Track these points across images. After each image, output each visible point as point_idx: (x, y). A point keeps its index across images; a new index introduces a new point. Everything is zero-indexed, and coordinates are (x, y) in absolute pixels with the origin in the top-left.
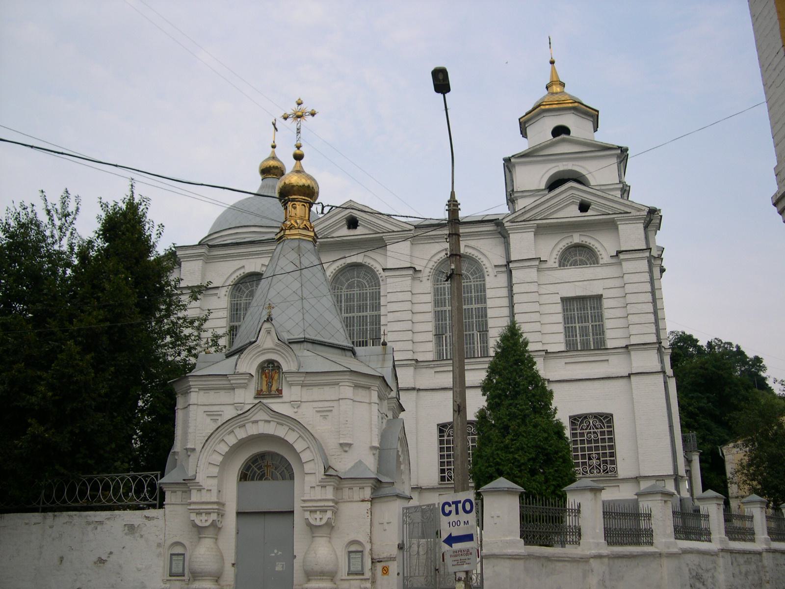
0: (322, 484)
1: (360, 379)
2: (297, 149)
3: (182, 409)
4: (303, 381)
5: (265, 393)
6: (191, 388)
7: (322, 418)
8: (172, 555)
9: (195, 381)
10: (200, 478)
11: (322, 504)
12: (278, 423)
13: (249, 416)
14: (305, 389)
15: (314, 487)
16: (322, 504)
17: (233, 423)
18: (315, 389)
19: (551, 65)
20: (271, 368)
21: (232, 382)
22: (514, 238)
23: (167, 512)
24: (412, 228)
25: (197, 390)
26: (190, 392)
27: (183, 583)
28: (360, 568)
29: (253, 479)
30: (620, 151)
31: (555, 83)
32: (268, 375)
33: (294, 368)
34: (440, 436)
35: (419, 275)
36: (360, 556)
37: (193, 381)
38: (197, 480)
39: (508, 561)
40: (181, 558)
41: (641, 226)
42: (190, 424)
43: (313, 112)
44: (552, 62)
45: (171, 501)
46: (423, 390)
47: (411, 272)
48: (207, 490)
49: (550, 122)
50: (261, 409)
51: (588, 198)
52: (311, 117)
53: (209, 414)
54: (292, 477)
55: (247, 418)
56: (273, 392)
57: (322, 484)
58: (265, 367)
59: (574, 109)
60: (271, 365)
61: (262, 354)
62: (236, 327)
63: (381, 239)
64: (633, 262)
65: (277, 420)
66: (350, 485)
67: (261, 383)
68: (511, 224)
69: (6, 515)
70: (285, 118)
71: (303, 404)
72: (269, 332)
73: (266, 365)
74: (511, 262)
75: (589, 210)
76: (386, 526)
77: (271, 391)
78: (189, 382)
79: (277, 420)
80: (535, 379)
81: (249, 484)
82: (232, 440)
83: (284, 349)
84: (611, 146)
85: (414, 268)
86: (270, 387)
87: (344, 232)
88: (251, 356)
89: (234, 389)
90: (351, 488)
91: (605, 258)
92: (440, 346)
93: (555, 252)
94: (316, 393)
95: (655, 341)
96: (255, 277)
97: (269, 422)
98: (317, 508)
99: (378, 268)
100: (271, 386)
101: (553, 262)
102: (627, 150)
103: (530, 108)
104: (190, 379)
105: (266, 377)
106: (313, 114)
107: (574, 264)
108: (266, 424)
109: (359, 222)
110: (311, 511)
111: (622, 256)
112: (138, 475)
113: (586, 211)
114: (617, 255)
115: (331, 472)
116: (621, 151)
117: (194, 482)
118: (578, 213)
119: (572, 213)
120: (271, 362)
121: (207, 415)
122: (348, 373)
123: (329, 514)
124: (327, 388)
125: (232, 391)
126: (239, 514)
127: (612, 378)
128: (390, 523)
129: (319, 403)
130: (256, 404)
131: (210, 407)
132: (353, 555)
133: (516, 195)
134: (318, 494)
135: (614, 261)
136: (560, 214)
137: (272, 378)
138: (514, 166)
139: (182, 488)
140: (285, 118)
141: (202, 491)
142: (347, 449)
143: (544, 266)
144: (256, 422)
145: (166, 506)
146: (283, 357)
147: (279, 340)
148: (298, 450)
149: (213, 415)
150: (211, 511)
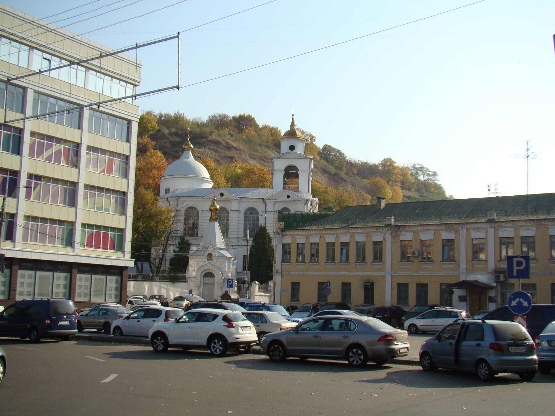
22: (268, 204)
31: (293, 125)
44: (293, 115)
63: (230, 201)
87: (220, 197)
99: (229, 209)
113: (289, 198)
115: (223, 277)
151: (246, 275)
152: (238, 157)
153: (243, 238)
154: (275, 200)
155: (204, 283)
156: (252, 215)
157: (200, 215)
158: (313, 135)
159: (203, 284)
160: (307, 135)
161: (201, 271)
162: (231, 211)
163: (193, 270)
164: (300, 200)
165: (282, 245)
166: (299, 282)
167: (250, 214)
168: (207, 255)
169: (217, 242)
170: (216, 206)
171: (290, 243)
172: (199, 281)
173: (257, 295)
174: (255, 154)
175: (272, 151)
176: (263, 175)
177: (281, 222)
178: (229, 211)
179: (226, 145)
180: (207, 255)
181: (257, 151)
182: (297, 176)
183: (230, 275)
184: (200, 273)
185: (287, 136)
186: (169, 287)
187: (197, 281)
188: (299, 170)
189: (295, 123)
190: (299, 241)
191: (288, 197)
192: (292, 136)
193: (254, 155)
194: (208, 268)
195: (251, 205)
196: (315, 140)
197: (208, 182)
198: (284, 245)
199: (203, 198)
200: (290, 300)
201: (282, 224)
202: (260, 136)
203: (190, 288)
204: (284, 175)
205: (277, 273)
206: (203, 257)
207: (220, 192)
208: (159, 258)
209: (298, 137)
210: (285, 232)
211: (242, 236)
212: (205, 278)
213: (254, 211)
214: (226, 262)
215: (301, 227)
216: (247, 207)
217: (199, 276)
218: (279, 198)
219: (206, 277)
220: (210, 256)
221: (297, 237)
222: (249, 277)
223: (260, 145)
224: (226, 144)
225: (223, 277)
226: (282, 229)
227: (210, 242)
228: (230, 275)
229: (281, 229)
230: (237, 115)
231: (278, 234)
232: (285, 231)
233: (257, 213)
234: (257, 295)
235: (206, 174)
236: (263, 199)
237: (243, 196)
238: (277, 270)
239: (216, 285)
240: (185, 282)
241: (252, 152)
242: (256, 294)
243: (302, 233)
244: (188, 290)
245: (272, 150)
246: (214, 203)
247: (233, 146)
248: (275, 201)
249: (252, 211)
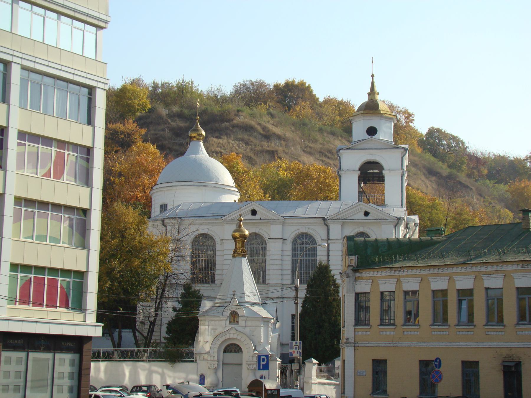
11: (253, 362)
16: (253, 362)
22: (331, 227)
31: (372, 92)
34: (292, 320)
35: (285, 241)
46: (285, 298)
47: (282, 240)
51: (368, 210)
54: (242, 351)
68: (331, 221)
85: (284, 239)
86: (234, 320)
87: (250, 217)
92: (294, 277)
99: (266, 237)
115: (256, 352)
136: (355, 217)
137: (235, 317)
144: (231, 334)
151: (296, 348)
152: (284, 151)
153: (291, 284)
154: (344, 219)
155: (225, 362)
156: (305, 246)
157: (218, 247)
158: (410, 111)
159: (223, 364)
160: (399, 112)
161: (219, 343)
162: (270, 240)
163: (206, 340)
164: (387, 219)
165: (354, 295)
166: (386, 360)
167: (302, 244)
168: (228, 314)
169: (246, 291)
170: (242, 231)
171: (369, 291)
172: (216, 359)
173: (315, 384)
174: (312, 145)
175: (340, 140)
176: (325, 179)
177: (352, 255)
178: (266, 239)
179: (262, 132)
180: (228, 315)
181: (316, 141)
182: (381, 178)
183: (268, 348)
184: (217, 346)
185: (362, 112)
186: (166, 371)
187: (212, 359)
189: (377, 89)
190: (383, 288)
191: (367, 214)
192: (371, 112)
193: (311, 147)
194: (231, 336)
195: (303, 230)
196: (413, 120)
197: (231, 192)
198: (357, 295)
199: (222, 218)
200: (371, 392)
201: (354, 259)
202: (320, 116)
203: (199, 373)
204: (359, 177)
205: (348, 343)
206: (222, 318)
207: (251, 208)
208: (149, 321)
209: (382, 112)
210: (359, 272)
211: (289, 282)
212: (225, 354)
213: (308, 238)
214: (262, 325)
215: (387, 263)
216: (295, 232)
217: (216, 350)
218: (352, 215)
219: (228, 352)
220: (234, 315)
221: (380, 281)
222: (301, 351)
223: (321, 130)
224: (264, 131)
225: (256, 352)
226: (354, 267)
227: (234, 291)
228: (268, 348)
229: (352, 268)
230: (282, 82)
231: (348, 277)
232: (360, 271)
233: (314, 242)
234: (315, 384)
235: (227, 179)
236: (324, 219)
237: (290, 214)
238: (347, 339)
239: (245, 366)
240: (192, 361)
241: (307, 143)
242: (313, 382)
243: (388, 274)
244: (197, 375)
245: (340, 138)
246: (240, 226)
247: (274, 134)
248: (343, 222)
249: (306, 239)
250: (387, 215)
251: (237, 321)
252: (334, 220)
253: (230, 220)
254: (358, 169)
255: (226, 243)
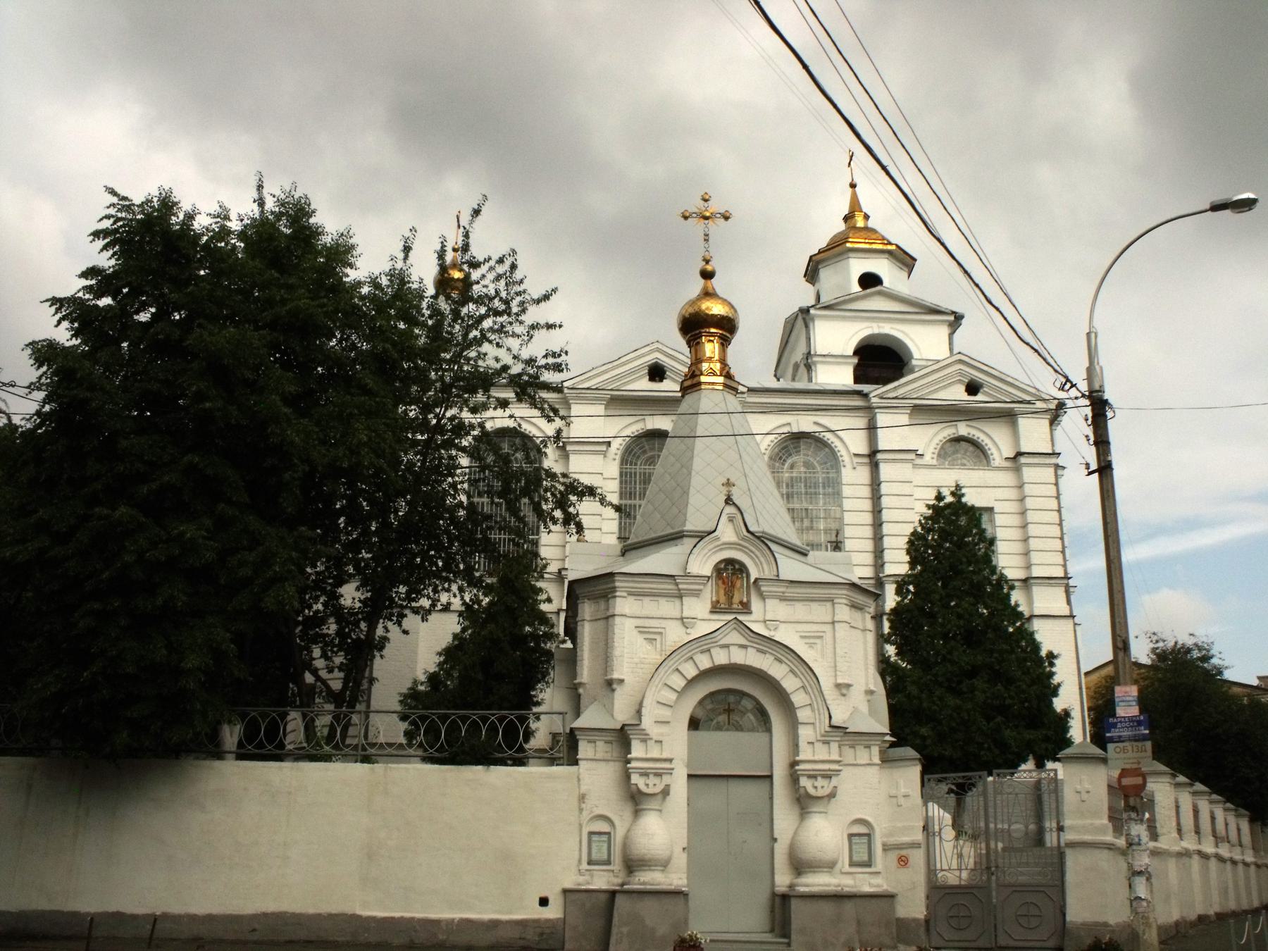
0: (823, 738)
1: (856, 596)
2: (497, 258)
3: (591, 621)
4: (783, 593)
5: (722, 606)
6: (615, 591)
7: (807, 646)
8: (591, 833)
9: (652, 583)
10: (647, 723)
11: (826, 766)
12: (759, 651)
13: (719, 637)
14: (785, 603)
15: (813, 743)
16: (826, 766)
17: (695, 646)
18: (799, 605)
19: (851, 189)
20: (730, 572)
21: (681, 586)
22: (882, 419)
23: (581, 770)
24: (745, 390)
25: (625, 594)
26: (615, 597)
27: (611, 874)
28: (865, 858)
29: (708, 729)
30: (952, 318)
32: (726, 580)
33: (768, 573)
36: (866, 841)
37: (622, 581)
38: (643, 726)
39: (1106, 851)
40: (605, 838)
41: (1046, 423)
42: (616, 644)
43: (728, 215)
44: (853, 186)
45: (814, 756)
48: (656, 741)
49: (858, 266)
50: (735, 628)
52: (723, 220)
53: (641, 630)
55: (714, 640)
56: (735, 606)
57: (823, 738)
58: (721, 569)
59: (890, 252)
60: (730, 567)
61: (721, 549)
62: (635, 506)
64: (1038, 469)
65: (757, 646)
66: (866, 743)
67: (717, 593)
69: (492, 767)
70: (686, 218)
71: (782, 626)
72: (731, 520)
73: (722, 566)
74: (879, 451)
75: (979, 394)
76: (902, 801)
77: (732, 604)
78: (614, 581)
79: (757, 646)
80: (1016, 614)
81: (703, 735)
82: (691, 672)
83: (753, 545)
84: (943, 310)
86: (730, 598)
87: (644, 385)
88: (706, 551)
89: (681, 597)
90: (852, 747)
91: (997, 460)
93: (933, 445)
94: (799, 611)
95: (1062, 575)
96: (660, 435)
97: (744, 647)
98: (818, 773)
100: (732, 597)
101: (929, 458)
102: (962, 317)
103: (823, 244)
104: (616, 578)
105: (724, 583)
106: (726, 218)
107: (952, 465)
108: (743, 651)
109: (667, 373)
110: (810, 777)
111: (1023, 460)
112: (431, 713)
114: (1015, 458)
115: (834, 722)
116: (955, 317)
117: (637, 728)
118: (965, 397)
119: (957, 394)
120: (730, 562)
121: (640, 632)
122: (847, 587)
123: (834, 781)
124: (814, 605)
125: (677, 602)
126: (690, 776)
127: (1054, 616)
128: (909, 796)
129: (805, 625)
130: (730, 621)
131: (646, 620)
132: (855, 840)
133: (815, 359)
134: (821, 753)
135: (1007, 464)
136: (941, 395)
137: (733, 586)
138: (813, 320)
139: (605, 736)
140: (686, 218)
141: (648, 742)
142: (844, 691)
143: (919, 461)
144: (727, 646)
145: (580, 762)
146: (750, 556)
147: (748, 531)
148: (789, 690)
149: (648, 632)
150: (661, 771)
159: (690, 776)
168: (707, 570)
188: (915, 357)
250: (1033, 391)
251: (741, 603)
252: (889, 398)
253: (588, 389)
254: (851, 352)
255: (575, 452)
